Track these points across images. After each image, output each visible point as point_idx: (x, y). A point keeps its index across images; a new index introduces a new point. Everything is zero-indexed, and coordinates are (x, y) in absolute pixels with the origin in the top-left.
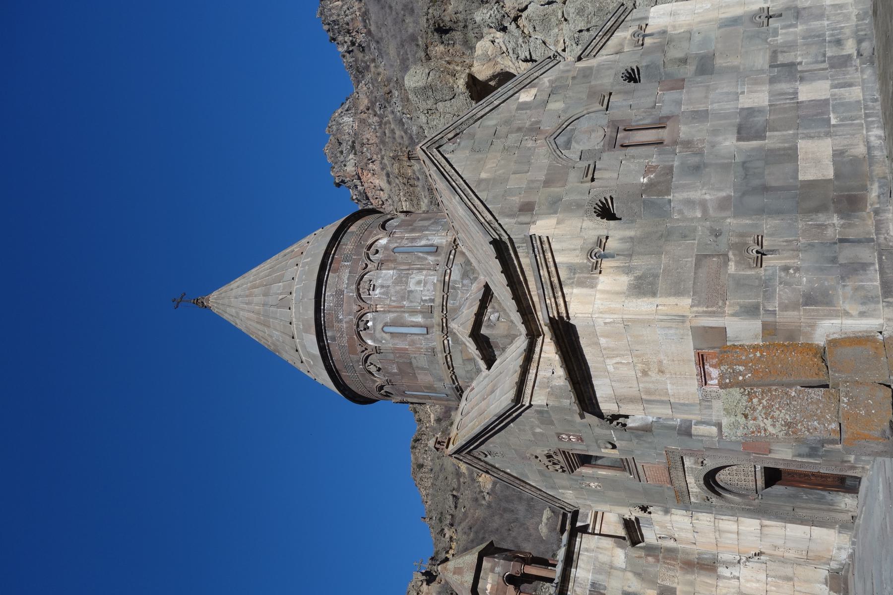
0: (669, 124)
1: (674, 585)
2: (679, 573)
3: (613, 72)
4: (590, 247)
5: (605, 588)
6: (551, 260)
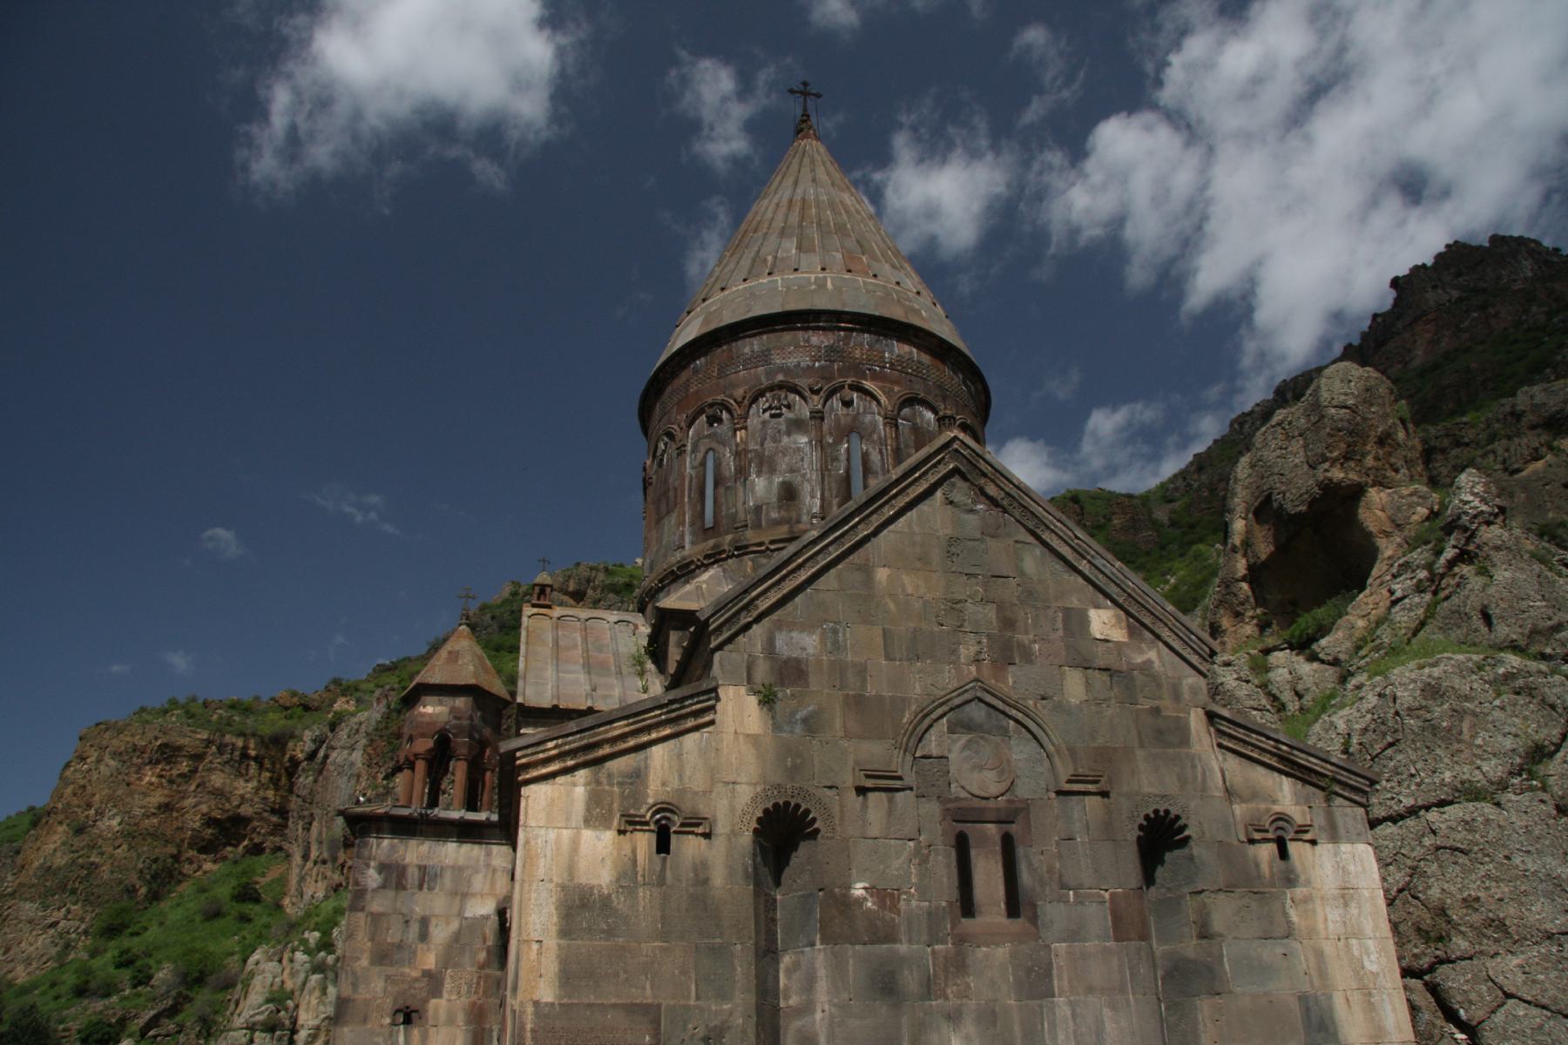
0: (1019, 924)
1: (445, 995)
2: (465, 1001)
3: (1172, 787)
4: (687, 806)
5: (431, 889)
6: (654, 735)
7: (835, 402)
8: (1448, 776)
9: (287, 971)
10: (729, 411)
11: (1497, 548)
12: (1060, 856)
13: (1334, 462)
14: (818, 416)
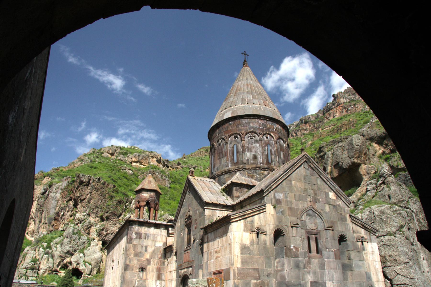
0: (319, 255)
1: (151, 265)
2: (155, 267)
3: (344, 230)
4: (262, 228)
6: (255, 213)
7: (265, 137)
8: (385, 230)
9: (37, 253)
10: (240, 136)
11: (392, 182)
12: (326, 242)
13: (355, 158)
14: (261, 140)
